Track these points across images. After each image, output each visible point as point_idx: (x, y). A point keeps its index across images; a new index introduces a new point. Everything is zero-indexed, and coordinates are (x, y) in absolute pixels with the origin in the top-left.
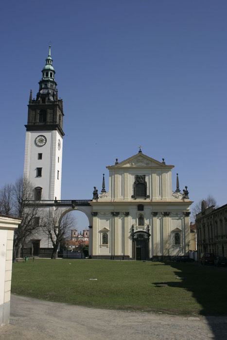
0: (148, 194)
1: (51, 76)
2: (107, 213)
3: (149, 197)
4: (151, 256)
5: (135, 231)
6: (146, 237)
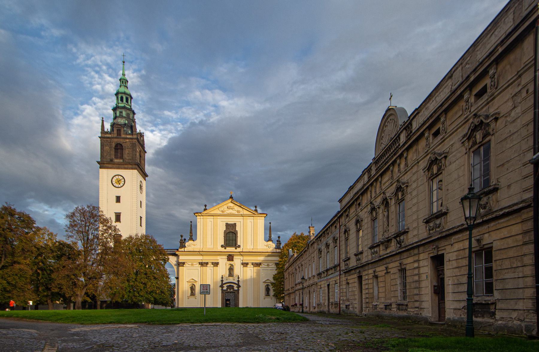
0: (239, 244)
1: (127, 101)
2: (195, 263)
3: (239, 246)
5: (224, 282)
6: (236, 288)
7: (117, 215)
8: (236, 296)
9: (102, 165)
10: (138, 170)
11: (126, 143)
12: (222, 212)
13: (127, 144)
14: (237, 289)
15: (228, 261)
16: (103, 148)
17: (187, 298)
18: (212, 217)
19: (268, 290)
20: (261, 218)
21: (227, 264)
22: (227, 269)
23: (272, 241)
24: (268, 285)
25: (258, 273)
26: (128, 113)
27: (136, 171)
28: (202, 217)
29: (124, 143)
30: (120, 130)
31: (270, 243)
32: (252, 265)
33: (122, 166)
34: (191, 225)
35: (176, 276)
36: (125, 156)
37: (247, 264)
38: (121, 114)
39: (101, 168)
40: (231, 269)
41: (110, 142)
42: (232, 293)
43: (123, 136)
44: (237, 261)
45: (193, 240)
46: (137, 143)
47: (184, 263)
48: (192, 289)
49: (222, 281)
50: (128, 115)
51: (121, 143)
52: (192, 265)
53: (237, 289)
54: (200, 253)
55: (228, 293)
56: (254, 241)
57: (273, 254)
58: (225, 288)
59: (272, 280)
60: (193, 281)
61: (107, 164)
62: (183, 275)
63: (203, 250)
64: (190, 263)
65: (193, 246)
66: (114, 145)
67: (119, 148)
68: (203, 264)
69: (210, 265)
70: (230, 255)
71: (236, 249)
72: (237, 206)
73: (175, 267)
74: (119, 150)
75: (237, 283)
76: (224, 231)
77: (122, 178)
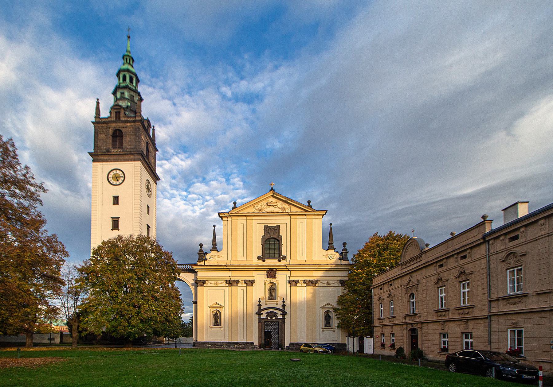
2: (219, 282)
3: (285, 258)
4: (287, 344)
6: (280, 316)
7: (114, 221)
8: (280, 326)
9: (96, 157)
10: (142, 163)
11: (126, 127)
12: (259, 210)
13: (128, 129)
14: (281, 317)
15: (268, 278)
16: (98, 136)
17: (209, 328)
18: (245, 218)
19: (328, 319)
20: (317, 217)
21: (267, 283)
22: (267, 290)
23: (335, 249)
24: (327, 312)
25: (314, 294)
26: (131, 95)
27: (140, 162)
28: (229, 219)
29: (124, 127)
30: (119, 112)
31: (332, 252)
32: (305, 283)
33: (122, 158)
34: (214, 230)
35: (194, 300)
36: (125, 145)
37: (297, 282)
38: (123, 96)
39: (94, 161)
40: (272, 290)
41: (106, 128)
42: (274, 322)
43: (123, 119)
44: (282, 279)
45: (217, 251)
46: (141, 128)
47: (204, 282)
48: (217, 317)
49: (260, 306)
50: (132, 97)
51: (120, 129)
52: (216, 284)
53: (281, 317)
54: (227, 268)
55: (269, 322)
56: (307, 249)
57: (336, 268)
58: (264, 316)
59: (335, 305)
60: (218, 306)
61: (101, 155)
62: (203, 298)
63: (231, 264)
64: (213, 282)
65: (217, 259)
66: (111, 132)
67: (118, 135)
68: (231, 283)
69: (242, 283)
70: (271, 270)
71: (280, 261)
72: (281, 202)
73: (192, 288)
74: (118, 138)
75: (282, 308)
76: (262, 236)
77: (123, 175)
